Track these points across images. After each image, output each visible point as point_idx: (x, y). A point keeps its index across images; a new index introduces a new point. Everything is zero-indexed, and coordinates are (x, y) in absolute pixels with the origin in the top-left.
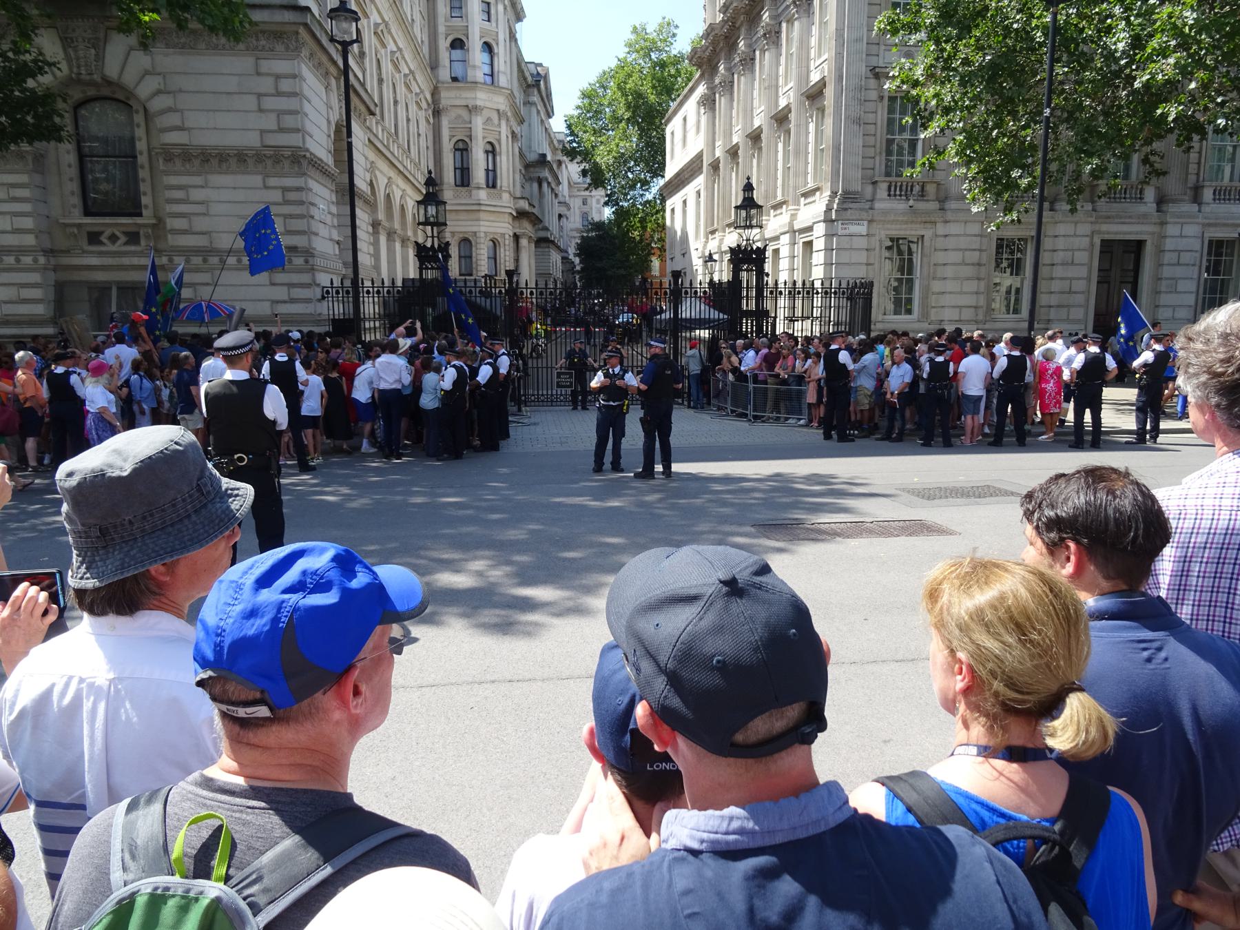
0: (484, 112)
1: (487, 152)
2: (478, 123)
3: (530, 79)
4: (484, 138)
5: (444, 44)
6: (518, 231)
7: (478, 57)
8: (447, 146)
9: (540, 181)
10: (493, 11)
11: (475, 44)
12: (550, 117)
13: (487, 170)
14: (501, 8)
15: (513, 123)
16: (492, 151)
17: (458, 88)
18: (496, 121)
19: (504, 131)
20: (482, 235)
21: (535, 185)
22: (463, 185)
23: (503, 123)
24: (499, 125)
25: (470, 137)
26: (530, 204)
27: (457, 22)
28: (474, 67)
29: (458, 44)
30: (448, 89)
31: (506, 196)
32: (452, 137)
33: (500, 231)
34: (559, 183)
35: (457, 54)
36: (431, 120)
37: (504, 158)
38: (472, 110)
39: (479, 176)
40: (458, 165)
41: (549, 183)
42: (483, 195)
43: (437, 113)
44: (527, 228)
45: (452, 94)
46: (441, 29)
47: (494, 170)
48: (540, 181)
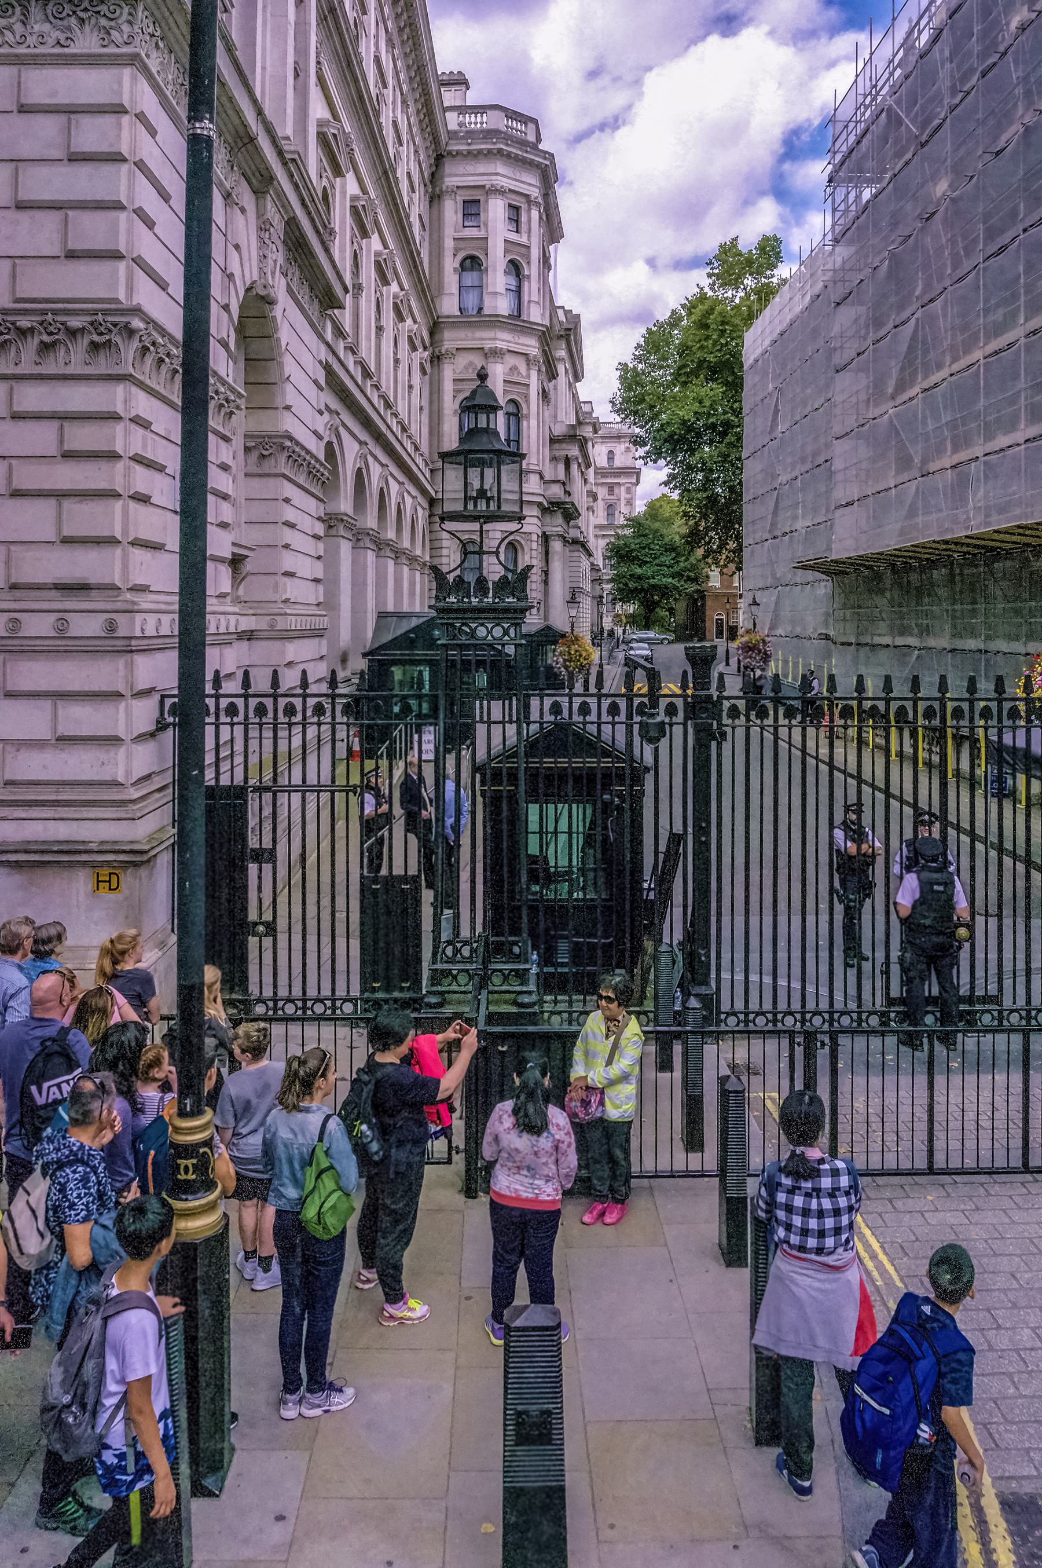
0: (507, 357)
2: (498, 372)
4: (505, 392)
5: (450, 263)
6: (547, 529)
7: (498, 280)
8: (450, 405)
10: (524, 218)
11: (497, 258)
14: (535, 214)
17: (469, 325)
18: (523, 368)
23: (534, 374)
24: (529, 376)
27: (473, 233)
28: (496, 293)
29: (472, 263)
32: (457, 391)
35: (470, 278)
37: (533, 423)
44: (556, 524)
45: (461, 334)
46: (449, 244)
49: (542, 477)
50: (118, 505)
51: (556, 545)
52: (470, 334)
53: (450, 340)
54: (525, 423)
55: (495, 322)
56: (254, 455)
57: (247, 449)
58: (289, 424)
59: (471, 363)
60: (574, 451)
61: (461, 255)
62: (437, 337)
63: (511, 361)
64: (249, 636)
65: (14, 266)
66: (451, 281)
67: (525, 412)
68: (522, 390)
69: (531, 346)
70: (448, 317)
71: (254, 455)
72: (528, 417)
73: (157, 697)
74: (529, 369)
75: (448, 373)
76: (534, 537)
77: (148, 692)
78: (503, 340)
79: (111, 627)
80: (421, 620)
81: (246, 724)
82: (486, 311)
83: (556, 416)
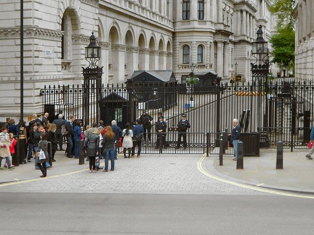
9: (242, 11)
13: (199, 11)
20: (195, 43)
21: (239, 13)
22: (187, 19)
26: (225, 26)
31: (209, 23)
33: (204, 40)
34: (255, 11)
39: (194, 14)
41: (247, 12)
42: (196, 25)
44: (220, 38)
47: (203, 11)
48: (242, 11)
49: (212, 23)
50: (32, 58)
51: (220, 45)
54: (205, 5)
56: (74, 40)
57: (72, 39)
58: (82, 32)
60: (245, 7)
64: (73, 79)
65: (15, 21)
71: (74, 40)
72: (206, 3)
73: (40, 90)
76: (209, 43)
77: (39, 89)
79: (31, 78)
80: (140, 73)
81: (50, 94)
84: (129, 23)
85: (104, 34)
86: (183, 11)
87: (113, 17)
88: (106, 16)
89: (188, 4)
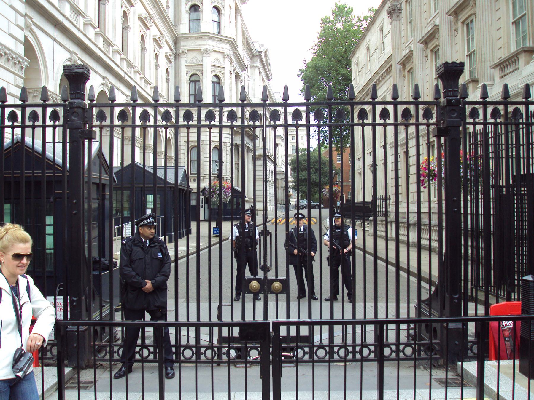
1: (214, 83)
2: (208, 61)
3: (254, 51)
5: (185, 8)
7: (207, 14)
8: (184, 79)
12: (269, 80)
15: (236, 65)
16: (218, 82)
19: (228, 67)
23: (228, 62)
25: (201, 72)
29: (195, 8)
30: (187, 38)
32: (188, 71)
35: (194, 15)
36: (172, 60)
38: (204, 52)
40: (192, 92)
43: (177, 56)
52: (194, 43)
53: (184, 46)
55: (207, 36)
59: (194, 57)
61: (189, 5)
62: (178, 45)
63: (215, 55)
66: (185, 17)
67: (222, 81)
68: (222, 70)
69: (226, 48)
70: (182, 34)
74: (224, 60)
75: (183, 62)
78: (211, 44)
82: (202, 31)
83: (255, 95)
84: (104, 78)
85: (47, 73)
86: (190, 95)
87: (72, 50)
88: (55, 40)
89: (198, 83)
